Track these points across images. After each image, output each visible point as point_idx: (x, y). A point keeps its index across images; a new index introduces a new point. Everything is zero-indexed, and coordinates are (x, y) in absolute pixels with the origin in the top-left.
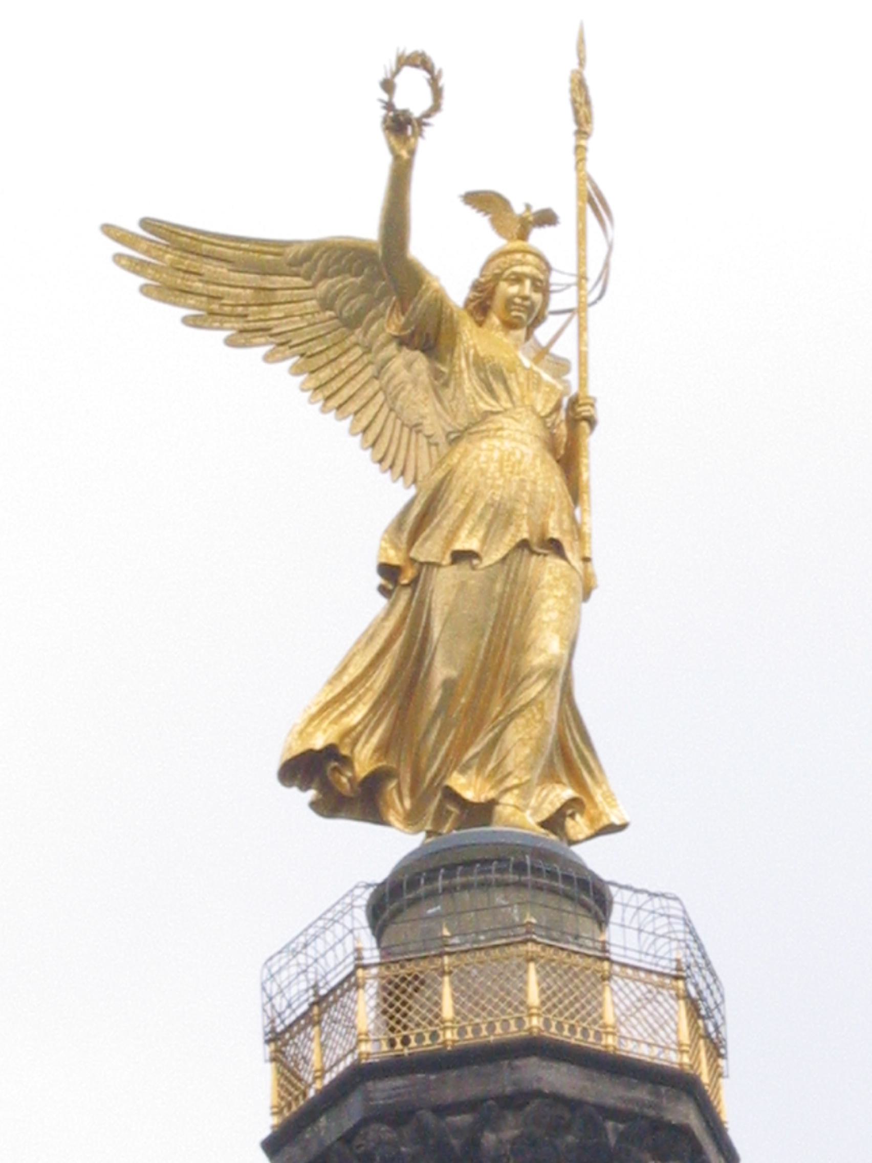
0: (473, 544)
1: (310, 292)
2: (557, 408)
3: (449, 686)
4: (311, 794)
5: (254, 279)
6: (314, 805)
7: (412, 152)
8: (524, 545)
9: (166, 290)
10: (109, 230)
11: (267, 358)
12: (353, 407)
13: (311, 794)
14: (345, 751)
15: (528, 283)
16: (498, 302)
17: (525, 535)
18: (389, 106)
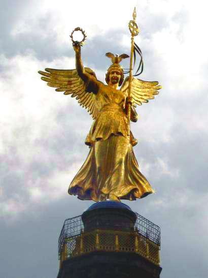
0: (101, 136)
1: (78, 81)
2: (123, 100)
3: (100, 168)
4: (77, 196)
5: (67, 79)
6: (78, 197)
7: (80, 50)
8: (112, 135)
9: (51, 84)
10: (40, 72)
11: (72, 96)
12: (88, 105)
13: (77, 196)
14: (80, 186)
15: (115, 74)
16: (110, 78)
17: (112, 132)
18: (73, 41)
